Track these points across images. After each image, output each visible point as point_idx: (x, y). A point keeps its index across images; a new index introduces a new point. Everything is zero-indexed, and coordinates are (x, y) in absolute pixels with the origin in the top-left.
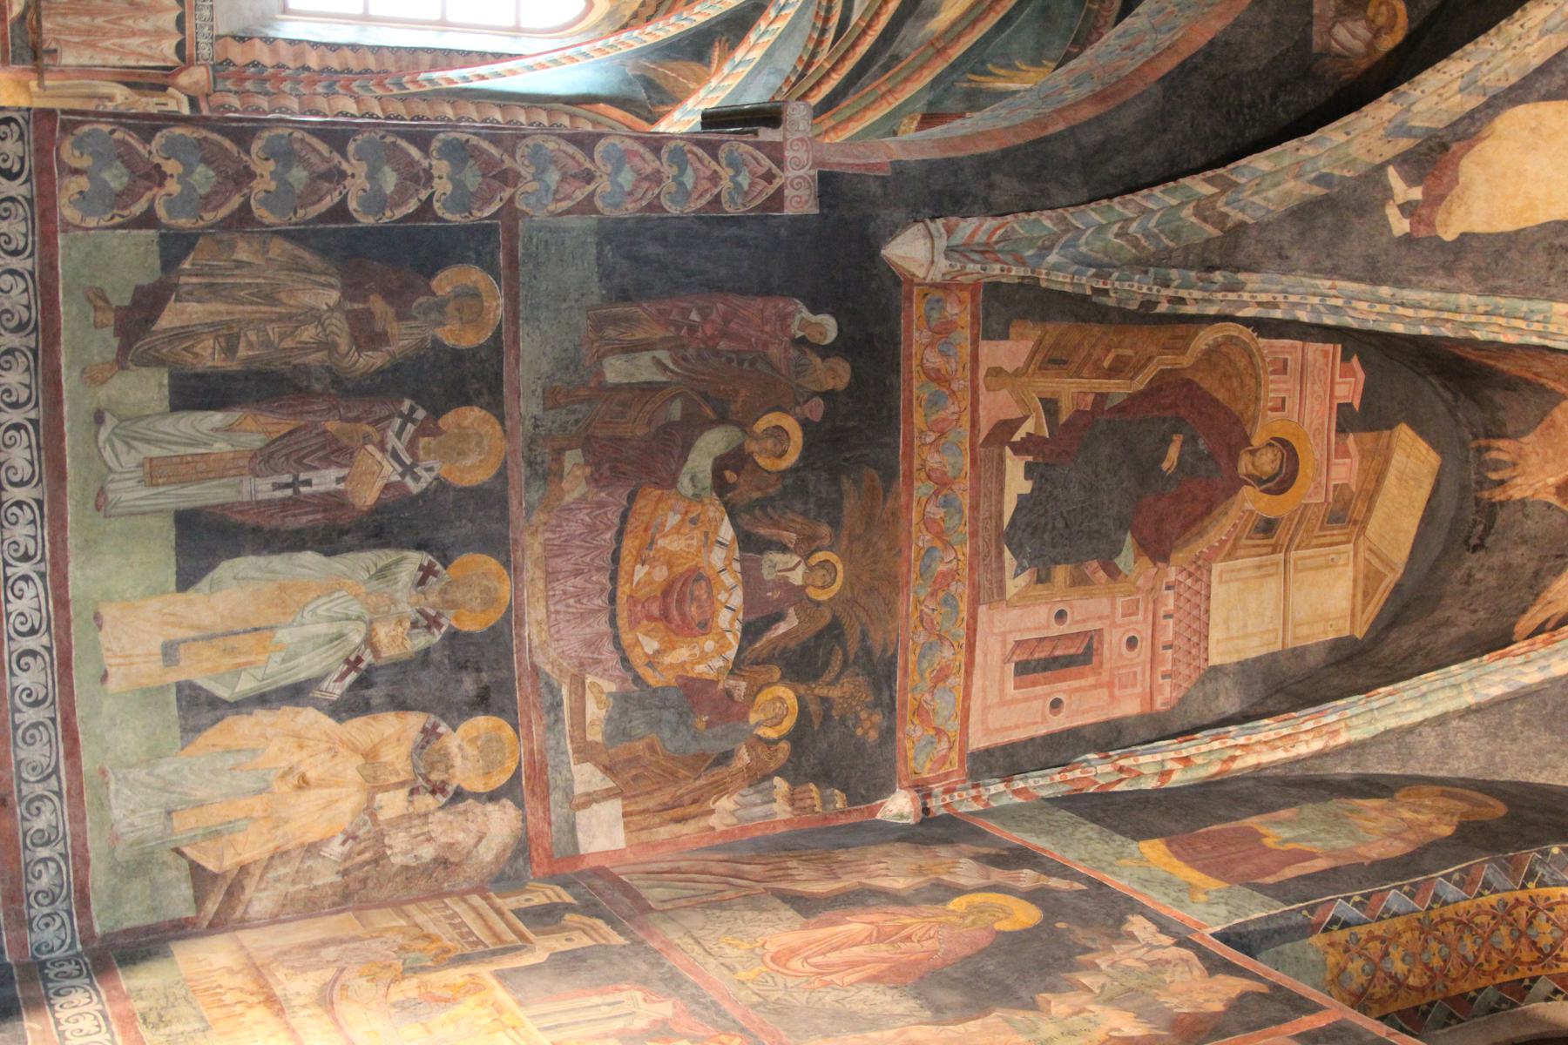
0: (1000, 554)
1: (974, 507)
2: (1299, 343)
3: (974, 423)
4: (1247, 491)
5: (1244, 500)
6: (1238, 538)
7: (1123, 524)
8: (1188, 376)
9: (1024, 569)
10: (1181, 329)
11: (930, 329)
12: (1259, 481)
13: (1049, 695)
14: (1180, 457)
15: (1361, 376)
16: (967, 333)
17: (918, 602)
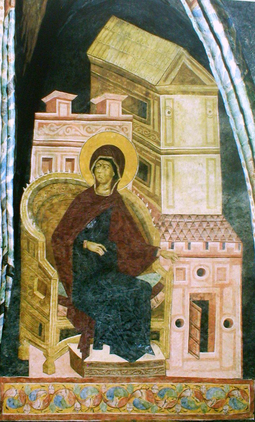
0: (141, 364)
1: (114, 380)
2: (34, 149)
3: (71, 381)
4: (120, 189)
5: (126, 189)
6: (149, 195)
7: (132, 281)
8: (50, 237)
9: (151, 349)
10: (24, 244)
11: (23, 405)
12: (115, 178)
13: (221, 329)
14: (97, 241)
15: (56, 94)
16: (26, 384)
17: (161, 410)
